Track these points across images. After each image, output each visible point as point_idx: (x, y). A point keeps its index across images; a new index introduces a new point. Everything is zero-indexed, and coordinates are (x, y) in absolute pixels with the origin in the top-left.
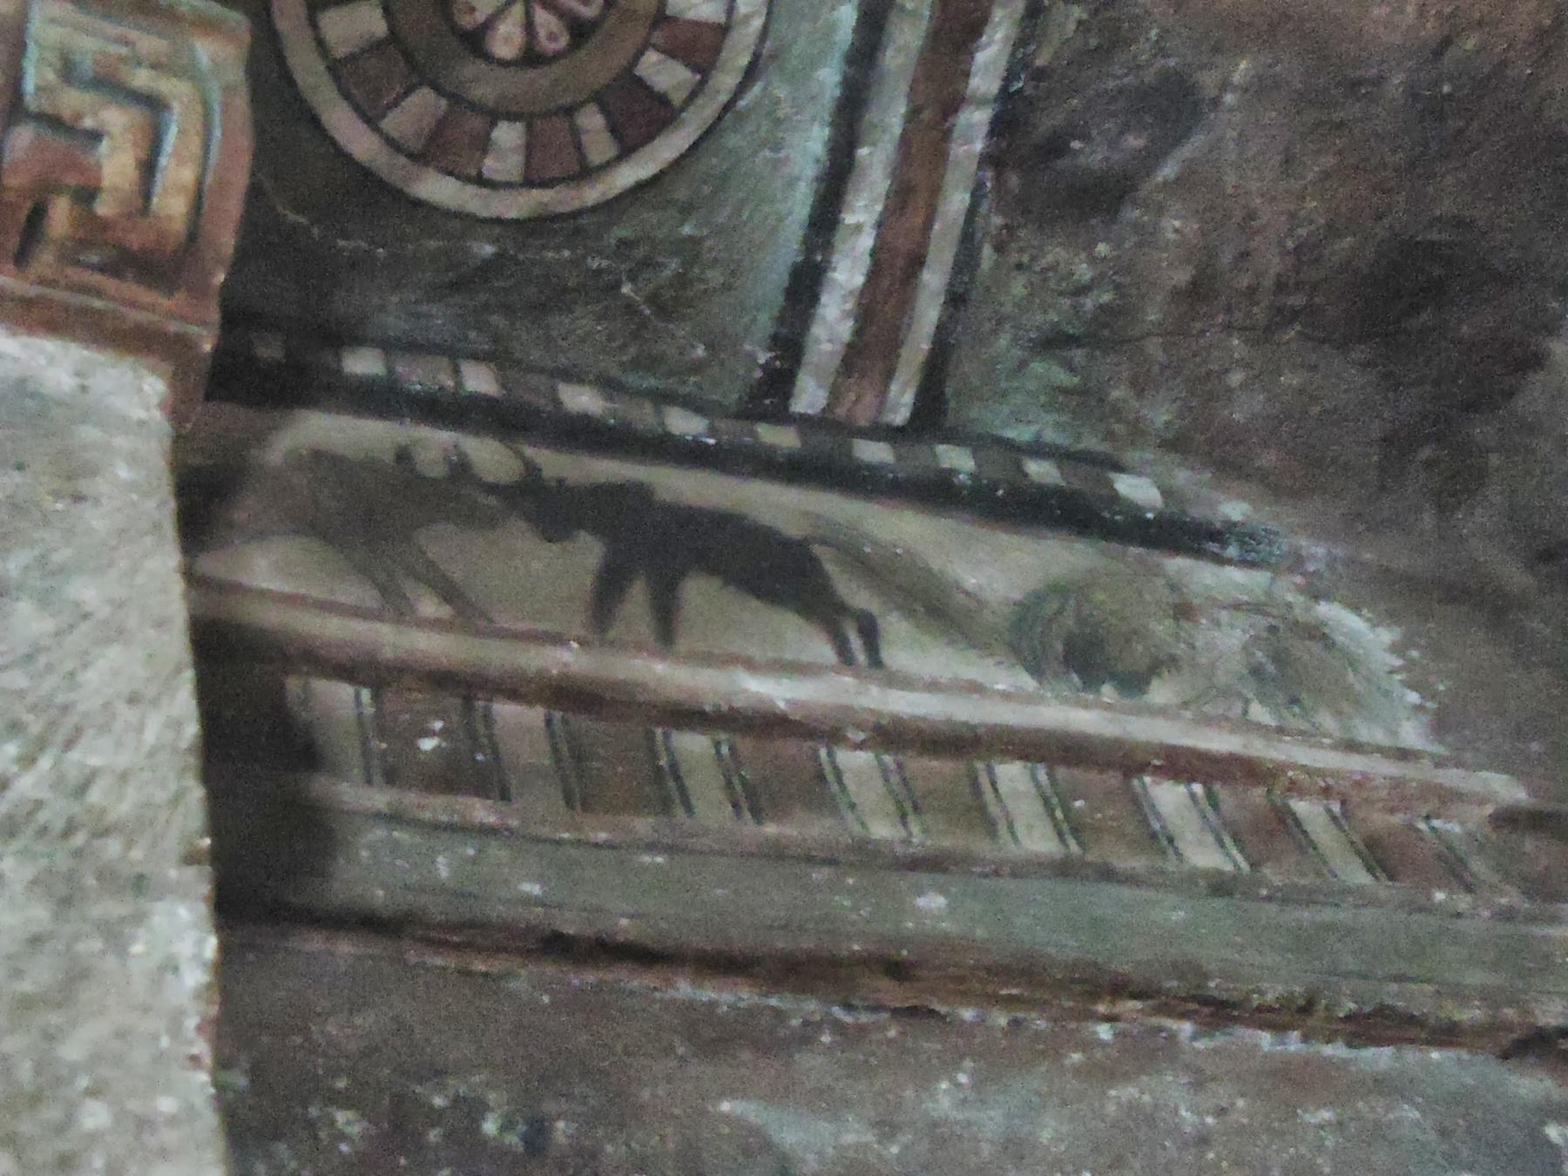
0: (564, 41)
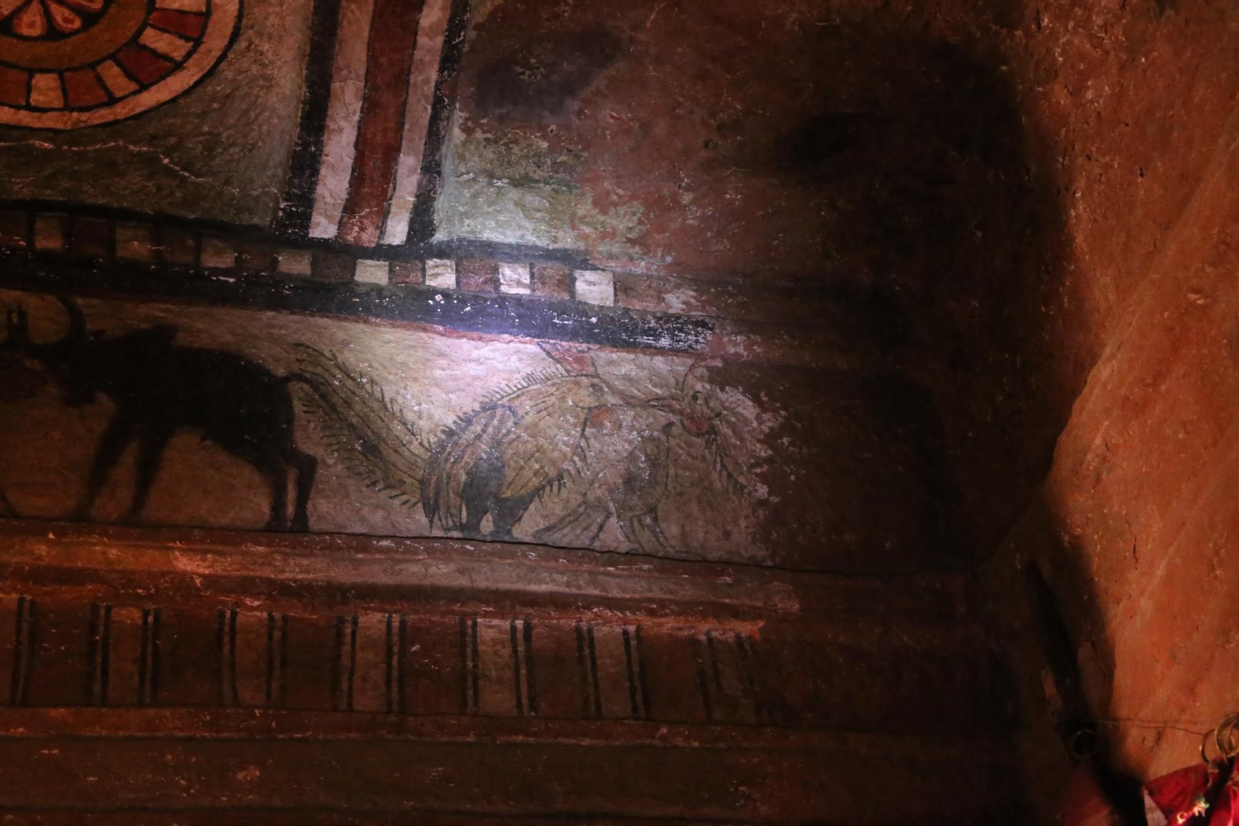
0: (77, 23)
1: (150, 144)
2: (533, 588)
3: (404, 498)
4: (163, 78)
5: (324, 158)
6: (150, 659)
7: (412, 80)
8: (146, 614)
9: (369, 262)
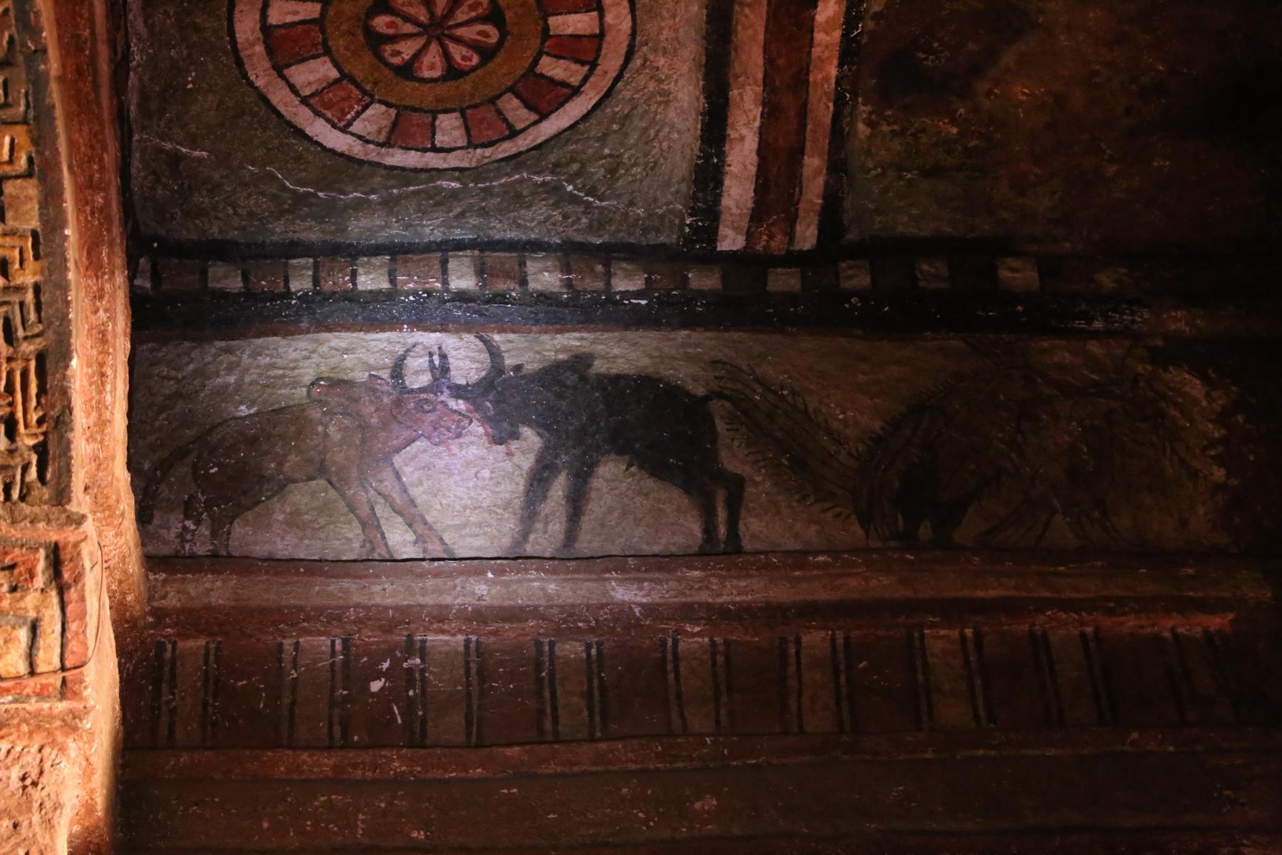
0: (475, 60)
1: (553, 173)
2: (980, 594)
3: (837, 510)
4: (561, 105)
5: (727, 169)
6: (596, 693)
7: (811, 79)
8: (589, 647)
9: (779, 270)
